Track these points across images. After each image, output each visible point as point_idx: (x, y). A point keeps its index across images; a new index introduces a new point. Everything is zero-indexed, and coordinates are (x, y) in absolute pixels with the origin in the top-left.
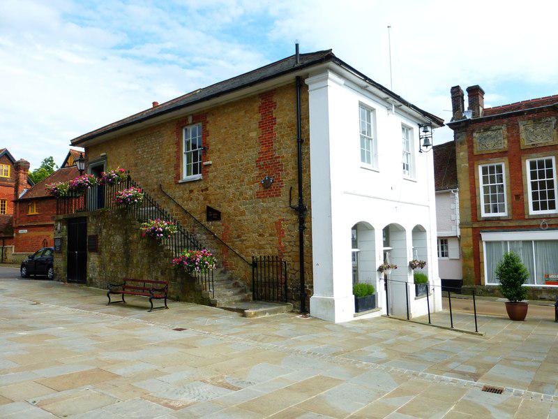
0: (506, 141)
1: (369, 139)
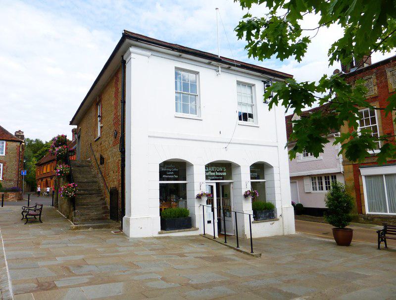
0: (376, 88)
1: (196, 96)
